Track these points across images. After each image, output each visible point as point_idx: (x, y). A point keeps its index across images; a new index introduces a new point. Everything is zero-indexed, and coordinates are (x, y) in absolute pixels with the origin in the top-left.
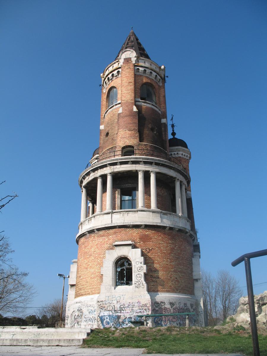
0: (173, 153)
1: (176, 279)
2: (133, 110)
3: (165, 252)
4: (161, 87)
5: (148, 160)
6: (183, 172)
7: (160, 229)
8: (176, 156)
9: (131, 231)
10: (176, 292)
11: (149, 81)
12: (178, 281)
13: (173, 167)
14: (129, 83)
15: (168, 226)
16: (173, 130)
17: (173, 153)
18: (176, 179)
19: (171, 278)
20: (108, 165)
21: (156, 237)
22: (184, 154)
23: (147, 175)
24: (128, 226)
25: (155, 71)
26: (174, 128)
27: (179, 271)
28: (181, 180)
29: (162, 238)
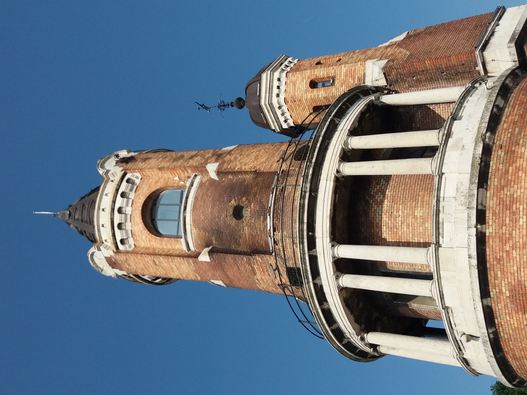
2: (208, 262)
4: (144, 176)
7: (488, 250)
8: (285, 108)
9: (507, 329)
14: (156, 265)
15: (473, 231)
17: (282, 119)
18: (339, 176)
20: (344, 343)
21: (515, 268)
23: (343, 266)
24: (492, 336)
25: (114, 202)
28: (338, 159)
29: (514, 248)
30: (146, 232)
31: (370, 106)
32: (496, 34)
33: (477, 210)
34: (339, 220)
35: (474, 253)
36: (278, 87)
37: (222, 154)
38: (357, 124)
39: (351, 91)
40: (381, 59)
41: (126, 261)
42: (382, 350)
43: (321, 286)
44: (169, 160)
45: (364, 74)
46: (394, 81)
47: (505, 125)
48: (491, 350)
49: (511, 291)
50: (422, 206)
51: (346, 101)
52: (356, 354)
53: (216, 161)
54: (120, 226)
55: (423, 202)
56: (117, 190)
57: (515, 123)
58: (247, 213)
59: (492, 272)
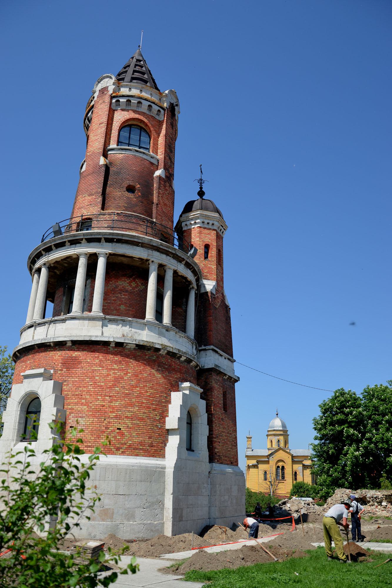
0: (188, 223)
1: (118, 431)
3: (103, 384)
5: (91, 235)
6: (165, 248)
10: (113, 454)
11: (137, 116)
12: (122, 434)
13: (140, 243)
15: (111, 340)
16: (201, 188)
17: (188, 223)
18: (150, 262)
19: (107, 428)
22: (206, 221)
23: (92, 260)
24: (48, 344)
25: (146, 100)
26: (202, 184)
27: (127, 417)
28: (160, 262)
29: (101, 361)
30: (123, 120)
31: (190, 283)
32: (220, 357)
33: (123, 343)
34: (122, 258)
35: (98, 339)
36: (208, 223)
37: (170, 181)
38: (180, 274)
39: (200, 272)
40: (216, 290)
41: (104, 102)
42: (36, 276)
43: (80, 243)
44: (170, 142)
45: (209, 279)
46: (203, 297)
47: (170, 361)
48: (40, 342)
49: (76, 357)
50: (126, 310)
51: (194, 269)
52: (34, 258)
53: (166, 176)
54: (129, 101)
55: (129, 310)
56: (154, 103)
57: (170, 366)
58: (130, 195)
59: (86, 348)
